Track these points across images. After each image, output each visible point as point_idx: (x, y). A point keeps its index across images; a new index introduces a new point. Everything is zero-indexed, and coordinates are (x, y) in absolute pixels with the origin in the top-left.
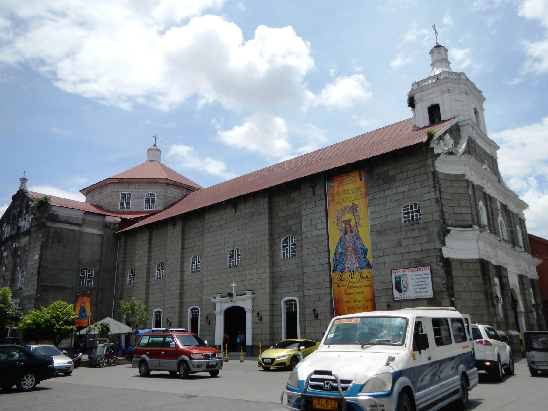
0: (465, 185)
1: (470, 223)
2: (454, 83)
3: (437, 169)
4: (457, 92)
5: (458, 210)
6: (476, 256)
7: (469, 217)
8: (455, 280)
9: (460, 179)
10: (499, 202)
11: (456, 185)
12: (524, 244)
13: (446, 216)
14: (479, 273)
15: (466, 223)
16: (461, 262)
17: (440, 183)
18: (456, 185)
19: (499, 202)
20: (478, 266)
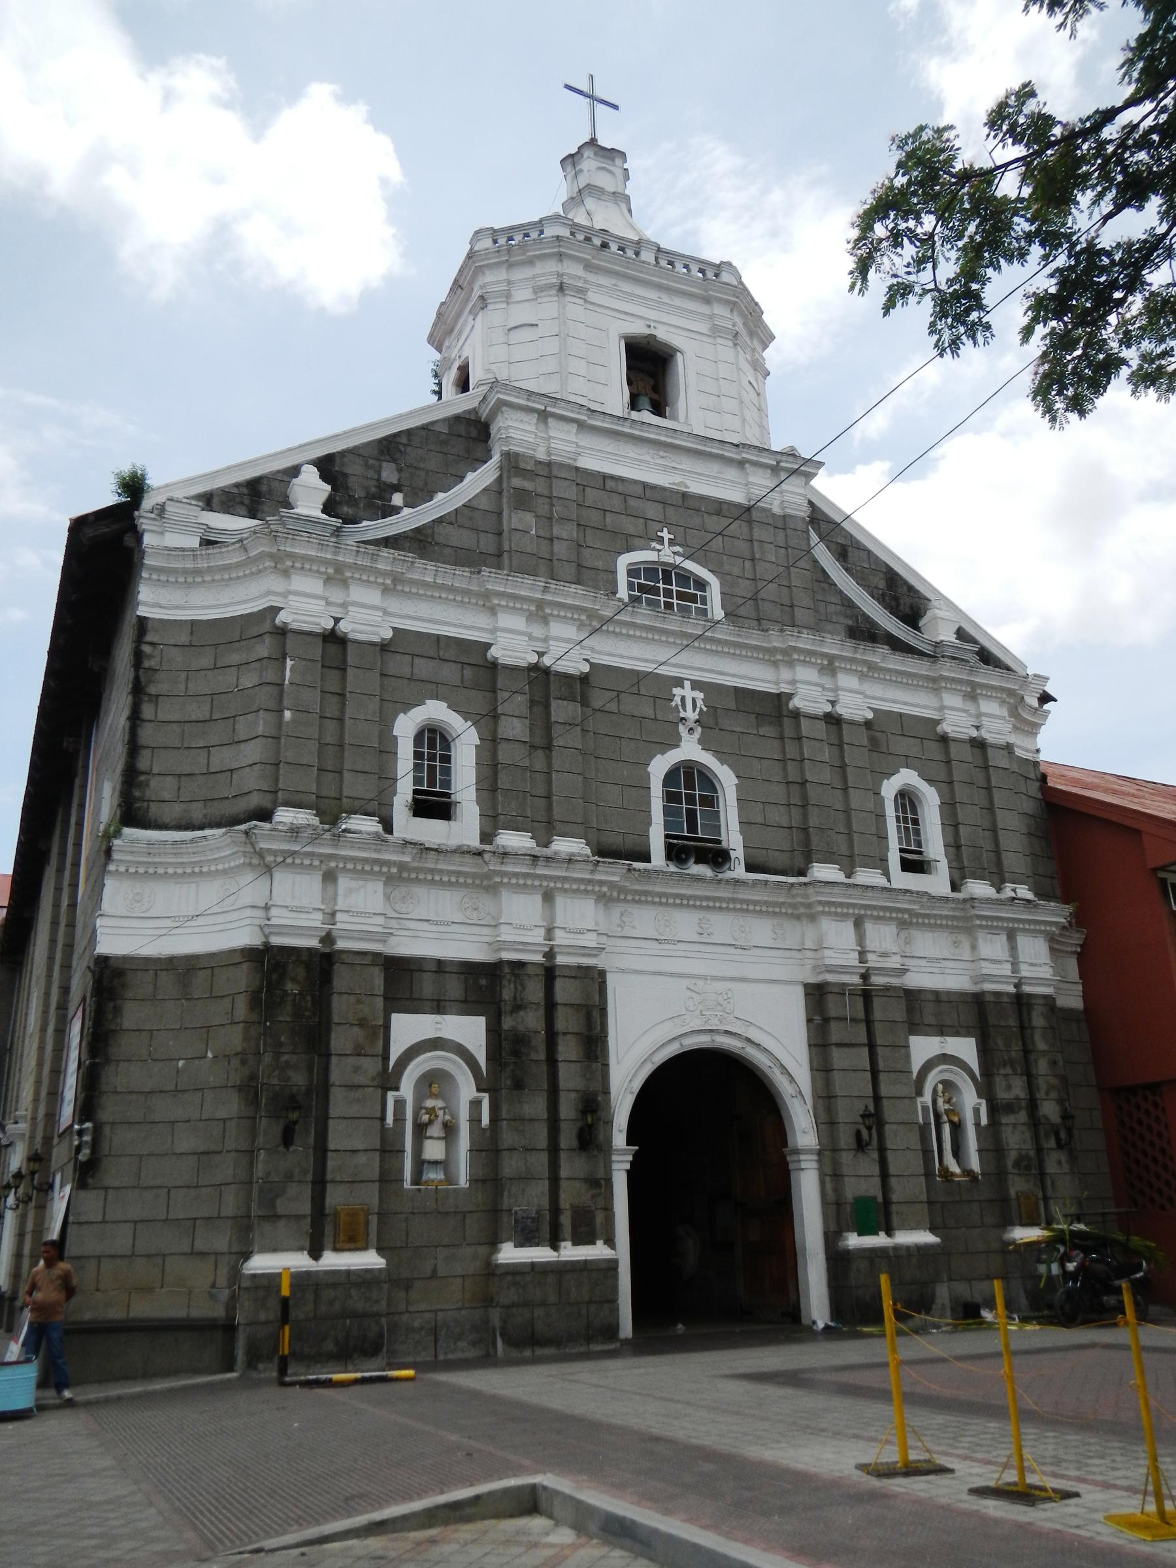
0: (263, 649)
1: (255, 801)
2: (511, 266)
3: (142, 611)
4: (522, 293)
5: (222, 758)
6: (244, 937)
7: (252, 780)
8: (124, 1045)
9: (255, 631)
10: (696, 685)
11: (235, 658)
12: (954, 846)
13: (160, 788)
14: (241, 1009)
15: (242, 806)
16: (184, 969)
17: (146, 664)
18: (235, 658)
19: (696, 685)
20: (243, 978)
